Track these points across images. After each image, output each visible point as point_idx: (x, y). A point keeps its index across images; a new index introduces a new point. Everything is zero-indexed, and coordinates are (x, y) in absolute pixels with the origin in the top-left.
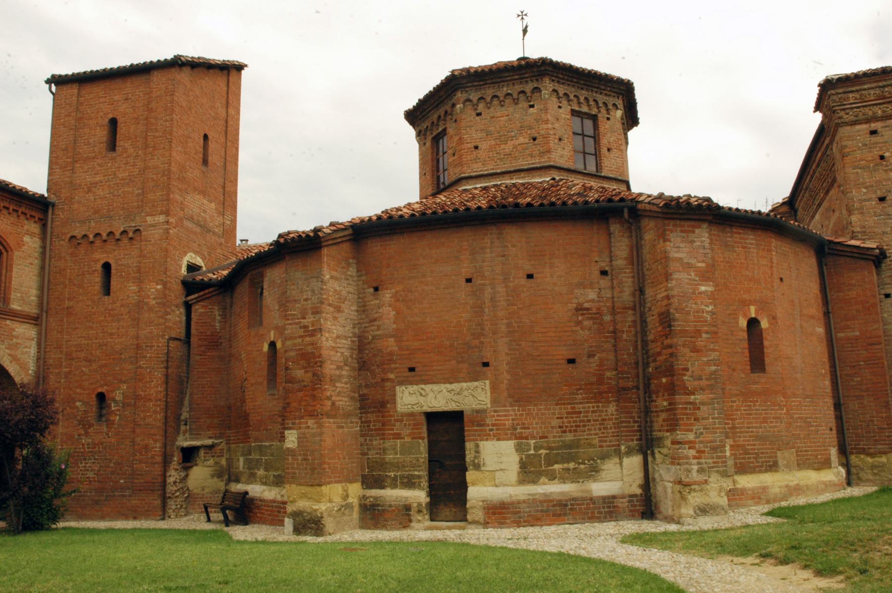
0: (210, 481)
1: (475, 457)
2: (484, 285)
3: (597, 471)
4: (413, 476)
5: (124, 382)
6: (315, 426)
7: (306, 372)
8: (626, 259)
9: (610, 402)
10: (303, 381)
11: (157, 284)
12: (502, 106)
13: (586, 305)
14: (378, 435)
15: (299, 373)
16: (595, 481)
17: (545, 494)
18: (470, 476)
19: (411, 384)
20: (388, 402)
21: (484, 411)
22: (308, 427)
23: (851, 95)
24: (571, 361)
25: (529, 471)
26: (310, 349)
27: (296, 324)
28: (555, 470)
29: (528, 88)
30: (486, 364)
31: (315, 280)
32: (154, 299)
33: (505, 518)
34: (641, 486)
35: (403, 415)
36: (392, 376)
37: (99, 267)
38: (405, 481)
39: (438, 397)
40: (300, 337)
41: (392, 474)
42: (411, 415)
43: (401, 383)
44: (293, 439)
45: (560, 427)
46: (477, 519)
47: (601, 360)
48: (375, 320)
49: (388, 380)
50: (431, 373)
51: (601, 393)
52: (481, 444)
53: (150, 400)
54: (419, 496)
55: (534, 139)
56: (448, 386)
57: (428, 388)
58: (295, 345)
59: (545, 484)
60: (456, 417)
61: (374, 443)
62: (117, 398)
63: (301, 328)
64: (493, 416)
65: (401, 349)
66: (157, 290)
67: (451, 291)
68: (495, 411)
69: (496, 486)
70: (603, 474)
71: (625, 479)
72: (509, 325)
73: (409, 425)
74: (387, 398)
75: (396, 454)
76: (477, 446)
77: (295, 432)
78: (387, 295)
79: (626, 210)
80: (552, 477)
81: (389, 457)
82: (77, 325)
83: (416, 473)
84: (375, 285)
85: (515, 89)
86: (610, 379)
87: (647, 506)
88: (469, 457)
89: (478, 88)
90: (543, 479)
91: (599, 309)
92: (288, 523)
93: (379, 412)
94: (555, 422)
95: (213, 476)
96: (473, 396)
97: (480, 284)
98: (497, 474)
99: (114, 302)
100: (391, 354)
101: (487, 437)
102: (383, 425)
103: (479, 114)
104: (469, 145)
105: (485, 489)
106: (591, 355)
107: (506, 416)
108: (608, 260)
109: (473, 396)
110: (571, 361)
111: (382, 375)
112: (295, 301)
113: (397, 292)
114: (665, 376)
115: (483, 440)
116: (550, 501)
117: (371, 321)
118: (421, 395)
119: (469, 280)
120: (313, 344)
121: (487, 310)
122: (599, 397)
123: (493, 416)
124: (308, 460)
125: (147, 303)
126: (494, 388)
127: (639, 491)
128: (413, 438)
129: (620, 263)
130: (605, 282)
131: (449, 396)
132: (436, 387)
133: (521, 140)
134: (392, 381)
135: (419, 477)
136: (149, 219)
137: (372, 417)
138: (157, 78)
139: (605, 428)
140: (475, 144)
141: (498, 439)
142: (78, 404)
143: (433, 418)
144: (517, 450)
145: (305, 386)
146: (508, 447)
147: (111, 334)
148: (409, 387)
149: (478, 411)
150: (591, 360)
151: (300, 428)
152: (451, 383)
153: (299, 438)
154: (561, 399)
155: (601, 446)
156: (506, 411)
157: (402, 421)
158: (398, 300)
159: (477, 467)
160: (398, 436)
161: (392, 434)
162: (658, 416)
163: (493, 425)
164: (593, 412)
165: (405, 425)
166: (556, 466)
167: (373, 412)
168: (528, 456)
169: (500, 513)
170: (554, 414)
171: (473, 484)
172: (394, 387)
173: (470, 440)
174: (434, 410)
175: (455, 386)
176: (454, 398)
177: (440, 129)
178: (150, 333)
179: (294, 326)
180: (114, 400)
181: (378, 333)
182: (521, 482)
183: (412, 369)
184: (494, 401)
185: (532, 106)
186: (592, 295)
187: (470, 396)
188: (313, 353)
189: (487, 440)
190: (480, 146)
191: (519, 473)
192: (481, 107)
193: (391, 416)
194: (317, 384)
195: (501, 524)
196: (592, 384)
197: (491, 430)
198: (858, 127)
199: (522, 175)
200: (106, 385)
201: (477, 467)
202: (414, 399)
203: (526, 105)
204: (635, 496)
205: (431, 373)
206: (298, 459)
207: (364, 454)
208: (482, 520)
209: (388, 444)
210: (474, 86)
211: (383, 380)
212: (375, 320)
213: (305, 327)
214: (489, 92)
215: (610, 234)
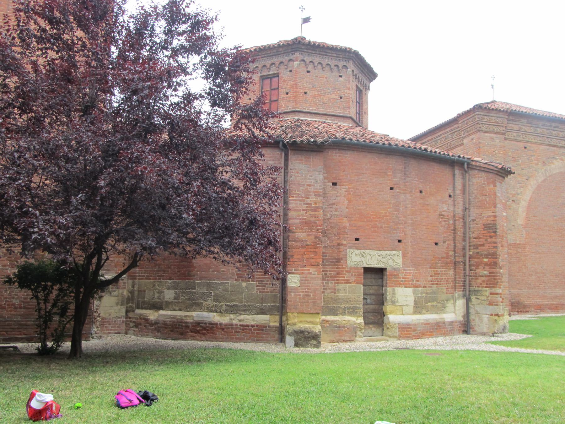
0: (116, 308)
1: (393, 297)
2: (400, 193)
3: (445, 307)
4: (356, 308)
6: (316, 273)
7: (308, 235)
8: (460, 190)
9: (450, 269)
10: (306, 241)
12: (324, 71)
13: (443, 213)
14: (333, 280)
15: (301, 235)
16: (444, 313)
17: (426, 320)
18: (388, 308)
19: (357, 249)
20: (342, 259)
21: (399, 269)
22: (310, 273)
23: (486, 117)
24: (436, 244)
25: (418, 308)
26: (313, 220)
27: (300, 201)
28: (428, 306)
29: (341, 64)
30: (399, 241)
31: (317, 173)
33: (410, 334)
34: (464, 316)
35: (351, 268)
36: (344, 242)
38: (351, 310)
39: (374, 259)
40: (304, 210)
41: (343, 306)
42: (357, 268)
43: (350, 248)
44: (296, 280)
45: (431, 281)
46: (395, 335)
47: (448, 245)
48: (333, 204)
49: (342, 245)
50: (369, 243)
51: (447, 263)
52: (396, 289)
54: (361, 320)
55: (341, 98)
56: (378, 252)
57: (367, 252)
58: (299, 216)
59: (424, 314)
60: (380, 272)
61: (330, 285)
63: (304, 204)
64: (403, 273)
65: (351, 225)
67: (382, 193)
68: (404, 270)
69: (403, 315)
70: (447, 309)
71: (457, 312)
72: (412, 220)
73: (355, 275)
74: (341, 256)
75: (346, 293)
76: (394, 290)
77: (298, 276)
78: (342, 189)
79: (466, 164)
80: (428, 311)
81: (341, 295)
83: (358, 306)
84: (334, 181)
85: (332, 63)
86: (451, 256)
87: (466, 328)
88: (389, 297)
90: (424, 311)
91: (448, 216)
92: (290, 340)
93: (335, 265)
94: (430, 279)
95: (117, 304)
96: (393, 260)
97: (398, 192)
98: (404, 307)
100: (345, 227)
101: (400, 285)
102: (337, 274)
103: (308, 72)
104: (302, 91)
105: (250, 317)
106: (444, 242)
107: (410, 273)
108: (452, 189)
109: (393, 260)
110: (436, 244)
111: (338, 241)
112: (299, 184)
113: (349, 188)
114: (487, 258)
115: (397, 287)
116: (428, 324)
117: (330, 205)
118: (363, 256)
119: (391, 189)
120: (315, 217)
121: (401, 208)
122: (446, 265)
123: (403, 273)
124: (309, 296)
126: (404, 256)
127: (462, 319)
128: (357, 283)
129: (458, 192)
130: (450, 201)
131: (380, 258)
132: (372, 252)
133: (334, 96)
134: (344, 245)
135: (359, 308)
137: (329, 268)
139: (449, 283)
140: (306, 91)
141: (406, 287)
143: (367, 270)
144: (414, 294)
145: (307, 245)
146: (410, 291)
148: (356, 251)
149: (394, 269)
150: (444, 245)
151: (303, 273)
152: (380, 250)
153: (301, 280)
154: (432, 265)
155: (447, 293)
156: (410, 270)
157: (350, 272)
158: (350, 194)
159: (393, 303)
160: (347, 282)
161: (344, 280)
162: (477, 279)
163: (403, 278)
164: (444, 274)
165: (352, 275)
166: (429, 304)
167: (329, 265)
168: (418, 297)
169: (407, 331)
170: (429, 273)
171: (391, 313)
172: (346, 249)
173: (390, 287)
174: (370, 266)
175: (383, 253)
176: (383, 260)
177: (271, 72)
179: (299, 202)
181: (336, 213)
182: (415, 313)
183: (357, 239)
184: (404, 264)
185: (341, 76)
186: (445, 208)
187: (390, 259)
188: (316, 223)
189: (399, 287)
190: (308, 93)
191: (414, 307)
192: (310, 67)
193: (343, 268)
194: (318, 244)
195: (407, 338)
196: (444, 258)
197: (402, 281)
198: (486, 134)
199: (333, 118)
201: (393, 303)
202: (359, 258)
203: (338, 74)
204: (460, 322)
205: (369, 243)
206: (300, 295)
207: (323, 292)
208: (397, 335)
209: (341, 286)
210: (308, 52)
211: (338, 244)
212: (333, 204)
213: (308, 204)
214: (317, 59)
215: (454, 175)
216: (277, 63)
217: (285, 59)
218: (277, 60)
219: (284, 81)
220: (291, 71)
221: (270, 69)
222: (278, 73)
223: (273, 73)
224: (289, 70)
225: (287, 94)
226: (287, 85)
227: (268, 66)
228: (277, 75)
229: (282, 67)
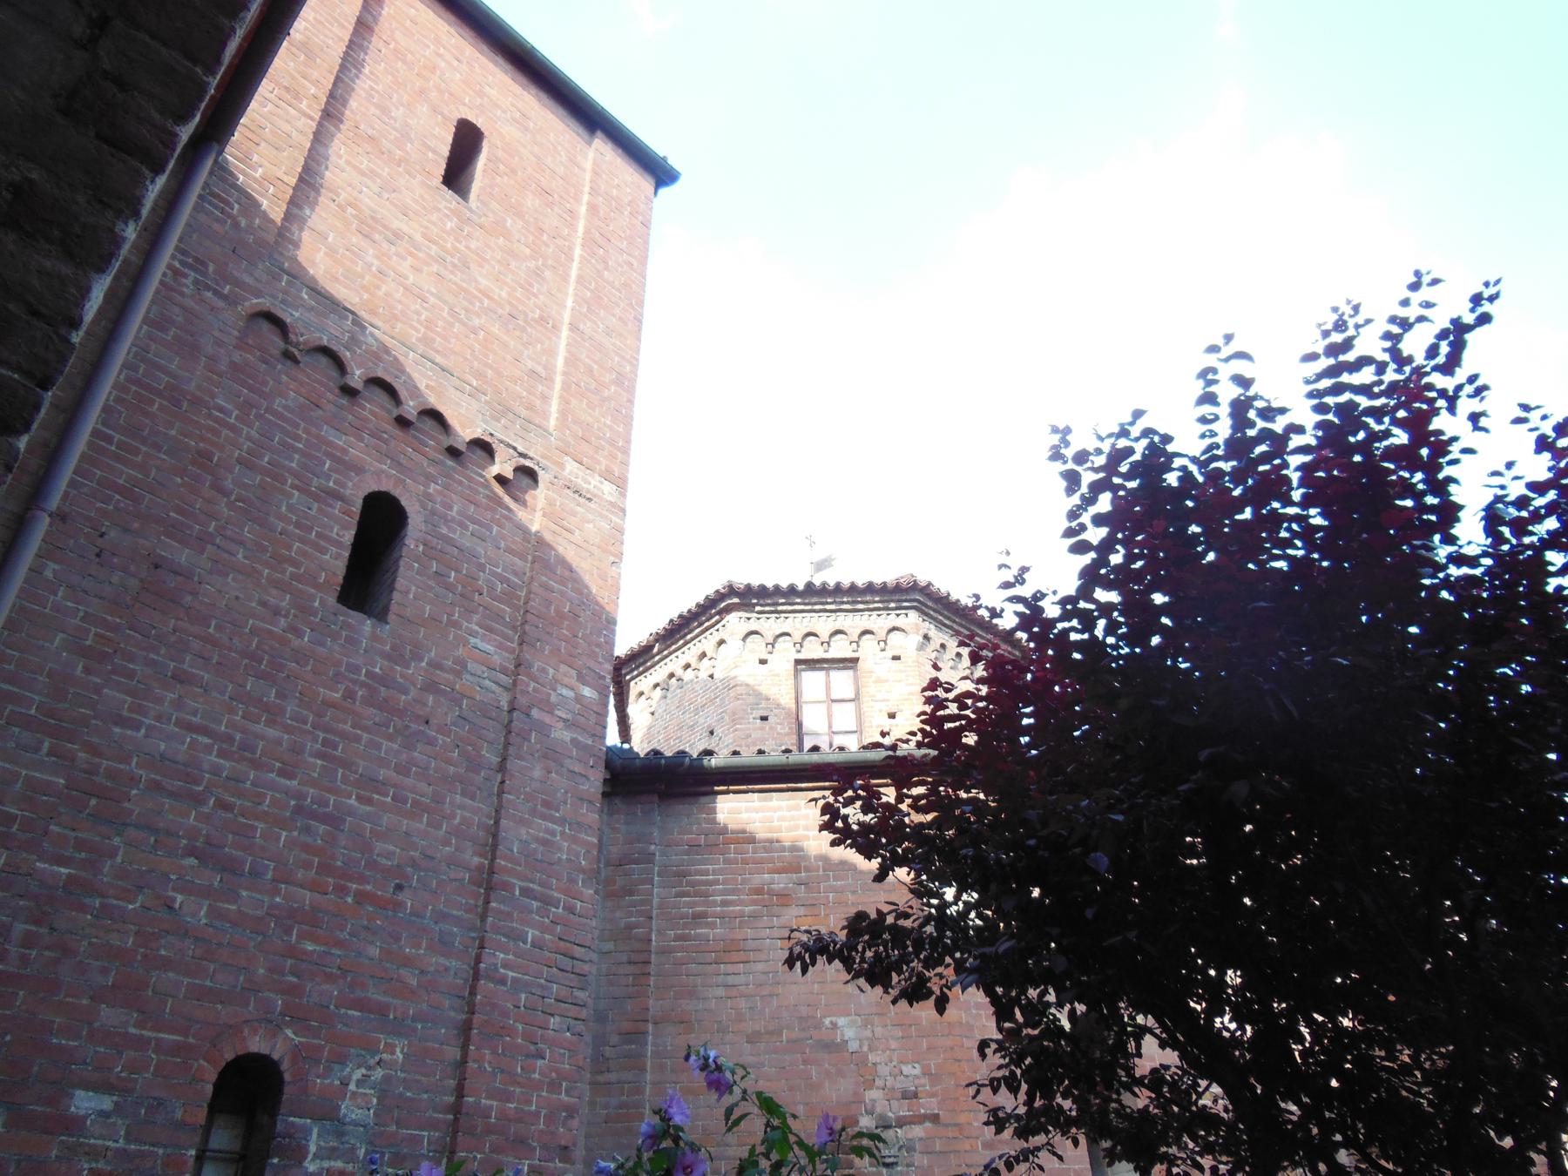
5: (399, 1028)
11: (581, 679)
32: (569, 724)
37: (357, 491)
53: (520, 1144)
62: (350, 1111)
66: (579, 698)
82: (188, 664)
99: (396, 656)
125: (544, 730)
136: (571, 466)
138: (601, 150)
142: (84, 1102)
147: (378, 786)
178: (545, 842)
180: (327, 1114)
200: (296, 1016)
217: (880, 622)
218: (853, 623)
222: (856, 660)
224: (890, 653)
227: (825, 636)
228: (850, 663)
229: (869, 645)
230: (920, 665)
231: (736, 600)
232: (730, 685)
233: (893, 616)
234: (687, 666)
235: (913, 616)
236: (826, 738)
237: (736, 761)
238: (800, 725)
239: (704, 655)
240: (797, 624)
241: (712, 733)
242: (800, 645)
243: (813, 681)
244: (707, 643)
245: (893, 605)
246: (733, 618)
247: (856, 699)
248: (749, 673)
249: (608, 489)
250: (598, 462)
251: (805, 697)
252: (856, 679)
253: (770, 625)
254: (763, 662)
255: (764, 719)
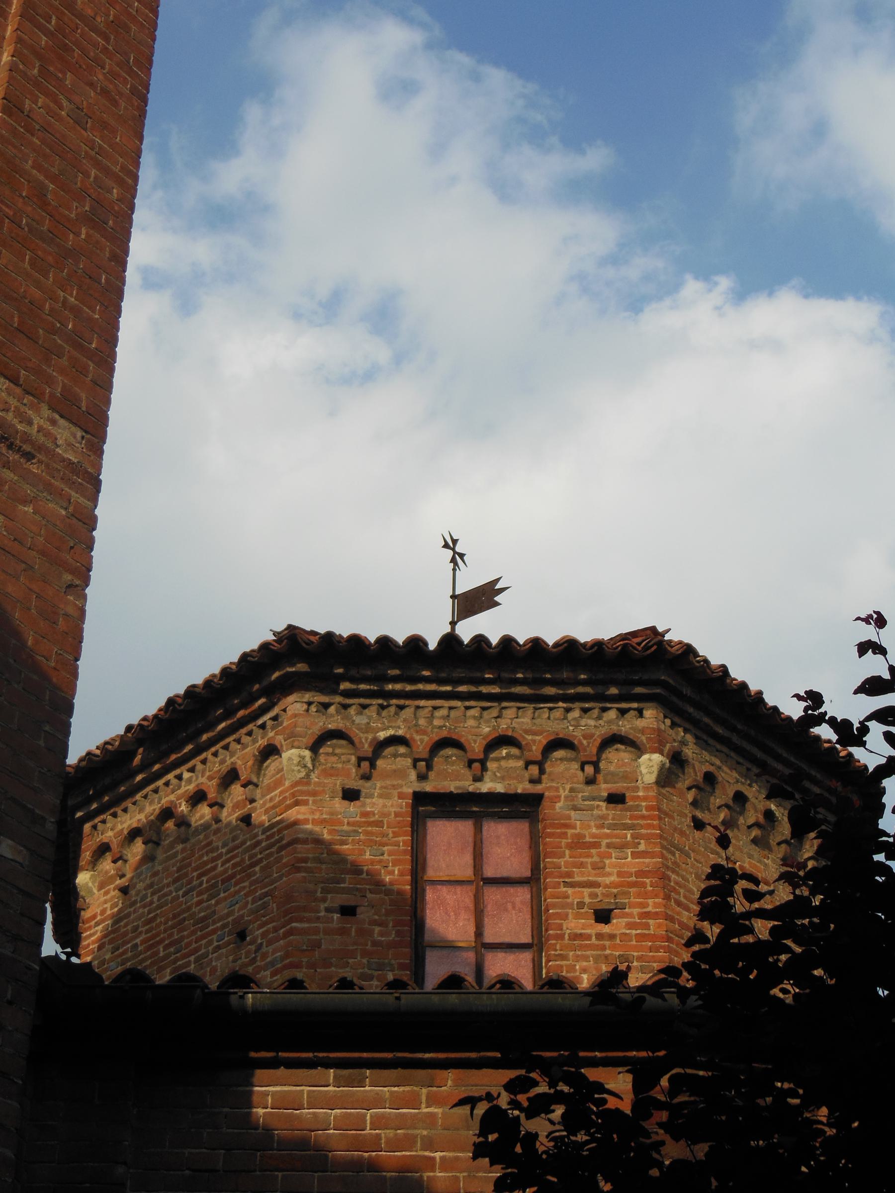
89: (706, 737)
177: (487, 786)
216: (536, 744)
217: (586, 725)
218: (533, 723)
219: (579, 844)
220: (616, 799)
221: (483, 763)
222: (536, 800)
223: (500, 788)
224: (604, 788)
225: (603, 916)
226: (599, 867)
227: (476, 747)
228: (523, 806)
230: (662, 814)
231: (302, 667)
232: (284, 837)
233: (612, 714)
234: (198, 797)
235: (651, 717)
236: (471, 956)
237: (294, 998)
238: (418, 925)
239: (231, 777)
240: (423, 721)
241: (242, 936)
242: (425, 765)
243: (448, 841)
244: (241, 754)
245: (614, 691)
246: (294, 705)
247: (533, 880)
248: (319, 815)
249: (65, 434)
250: (50, 381)
251: (431, 873)
252: (535, 840)
253: (371, 723)
254: (351, 795)
255: (348, 911)
